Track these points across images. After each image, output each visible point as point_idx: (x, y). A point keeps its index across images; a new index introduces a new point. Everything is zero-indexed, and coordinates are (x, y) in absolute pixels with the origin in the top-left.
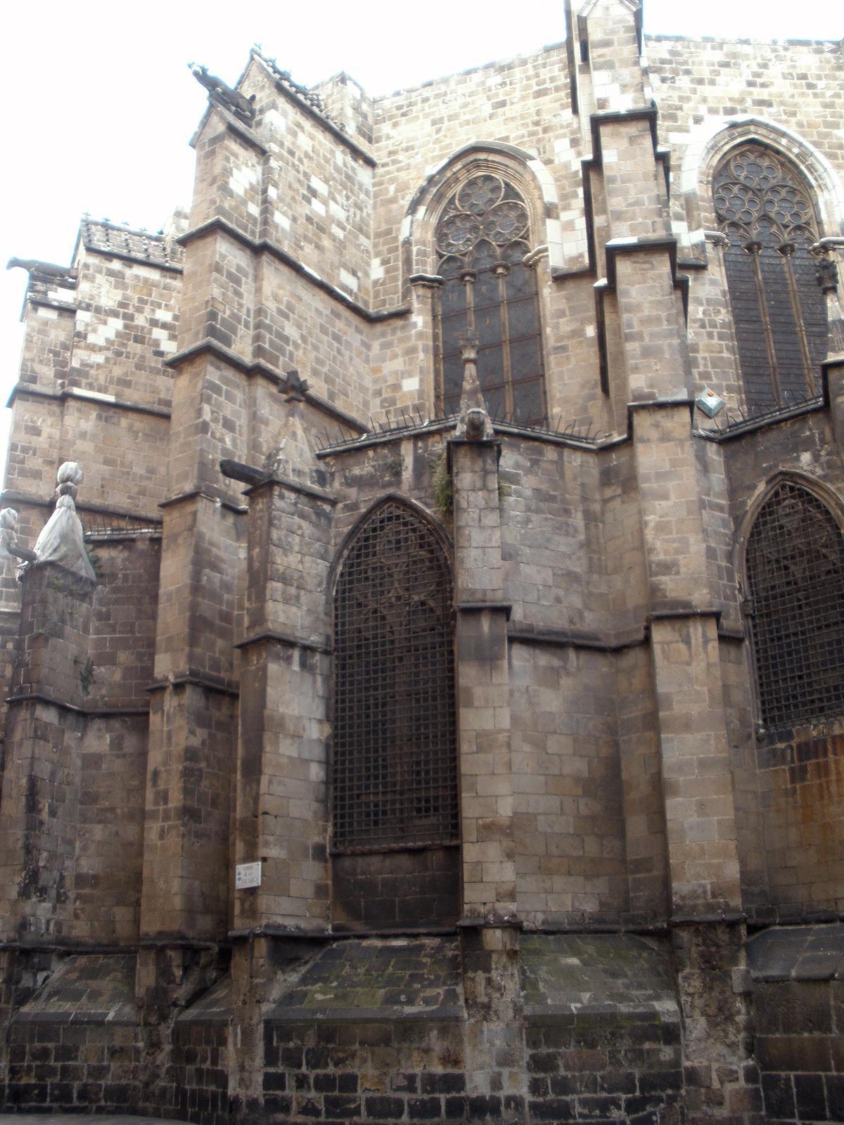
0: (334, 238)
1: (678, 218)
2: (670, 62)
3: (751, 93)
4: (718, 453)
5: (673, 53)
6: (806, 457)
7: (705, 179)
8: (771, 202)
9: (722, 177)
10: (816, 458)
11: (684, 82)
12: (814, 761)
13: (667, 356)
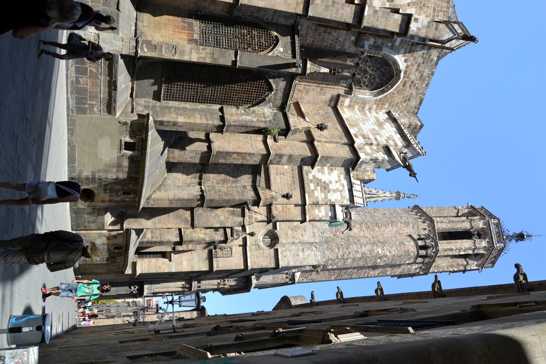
1: (375, 42)
2: (429, 58)
4: (290, 23)
5: (432, 59)
6: (282, 50)
10: (280, 53)
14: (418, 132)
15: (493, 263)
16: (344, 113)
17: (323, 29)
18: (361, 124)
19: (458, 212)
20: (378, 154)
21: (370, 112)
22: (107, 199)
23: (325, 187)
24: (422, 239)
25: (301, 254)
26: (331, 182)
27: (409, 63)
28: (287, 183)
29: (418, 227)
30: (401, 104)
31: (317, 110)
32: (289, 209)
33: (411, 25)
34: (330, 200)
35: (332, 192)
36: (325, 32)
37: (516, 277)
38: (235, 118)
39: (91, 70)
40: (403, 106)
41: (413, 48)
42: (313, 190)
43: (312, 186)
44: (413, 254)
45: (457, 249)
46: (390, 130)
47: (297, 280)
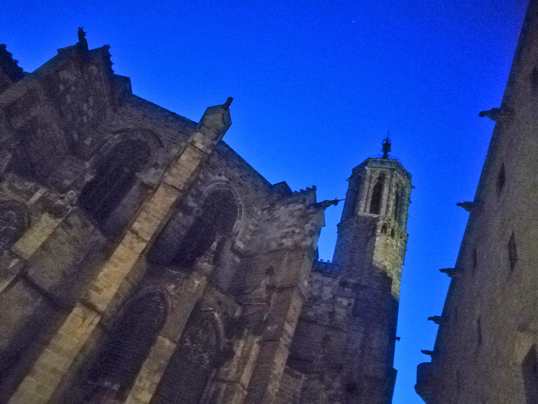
0: (82, 120)
1: (192, 196)
9: (214, 194)
20: (306, 229)
34: (330, 299)
42: (315, 315)
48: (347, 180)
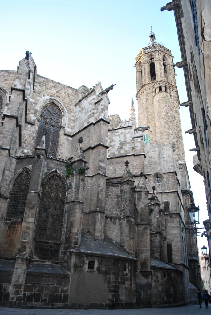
1: (32, 113)
2: (43, 83)
3: (57, 94)
4: (15, 161)
5: (44, 81)
7: (41, 108)
8: (53, 116)
9: (45, 108)
11: (44, 88)
12: (13, 226)
13: (8, 139)
14: (87, 88)
15: (168, 50)
16: (75, 131)
17: (22, 144)
18: (82, 121)
19: (139, 72)
20: (99, 109)
21: (75, 116)
22: (129, 282)
23: (123, 144)
24: (155, 90)
25: (166, 159)
26: (120, 141)
27: (46, 94)
28: (121, 166)
29: (148, 93)
30: (71, 99)
31: (74, 147)
32: (137, 165)
33: (18, 89)
34: (131, 140)
35: (126, 140)
36: (25, 143)
37: (170, 10)
38: (74, 195)
39: (37, 291)
40: (72, 97)
41: (36, 91)
42: (125, 151)
43: (123, 152)
44: (165, 95)
45: (160, 70)
46: (86, 103)
47: (183, 163)
48: (134, 67)
